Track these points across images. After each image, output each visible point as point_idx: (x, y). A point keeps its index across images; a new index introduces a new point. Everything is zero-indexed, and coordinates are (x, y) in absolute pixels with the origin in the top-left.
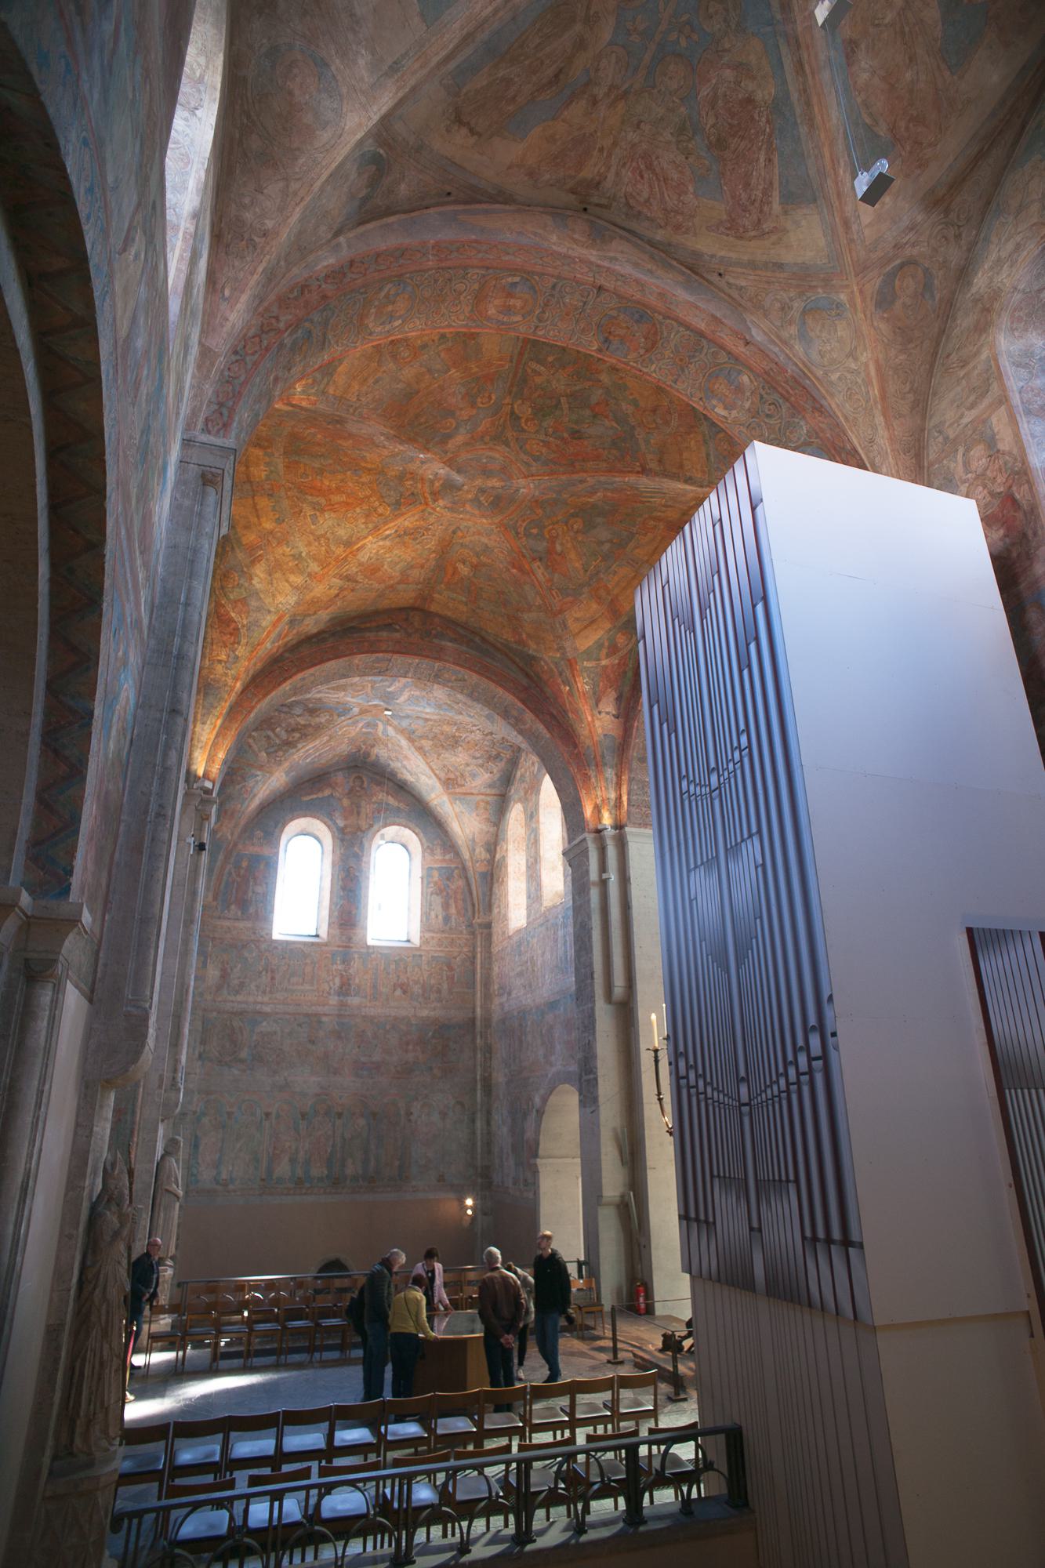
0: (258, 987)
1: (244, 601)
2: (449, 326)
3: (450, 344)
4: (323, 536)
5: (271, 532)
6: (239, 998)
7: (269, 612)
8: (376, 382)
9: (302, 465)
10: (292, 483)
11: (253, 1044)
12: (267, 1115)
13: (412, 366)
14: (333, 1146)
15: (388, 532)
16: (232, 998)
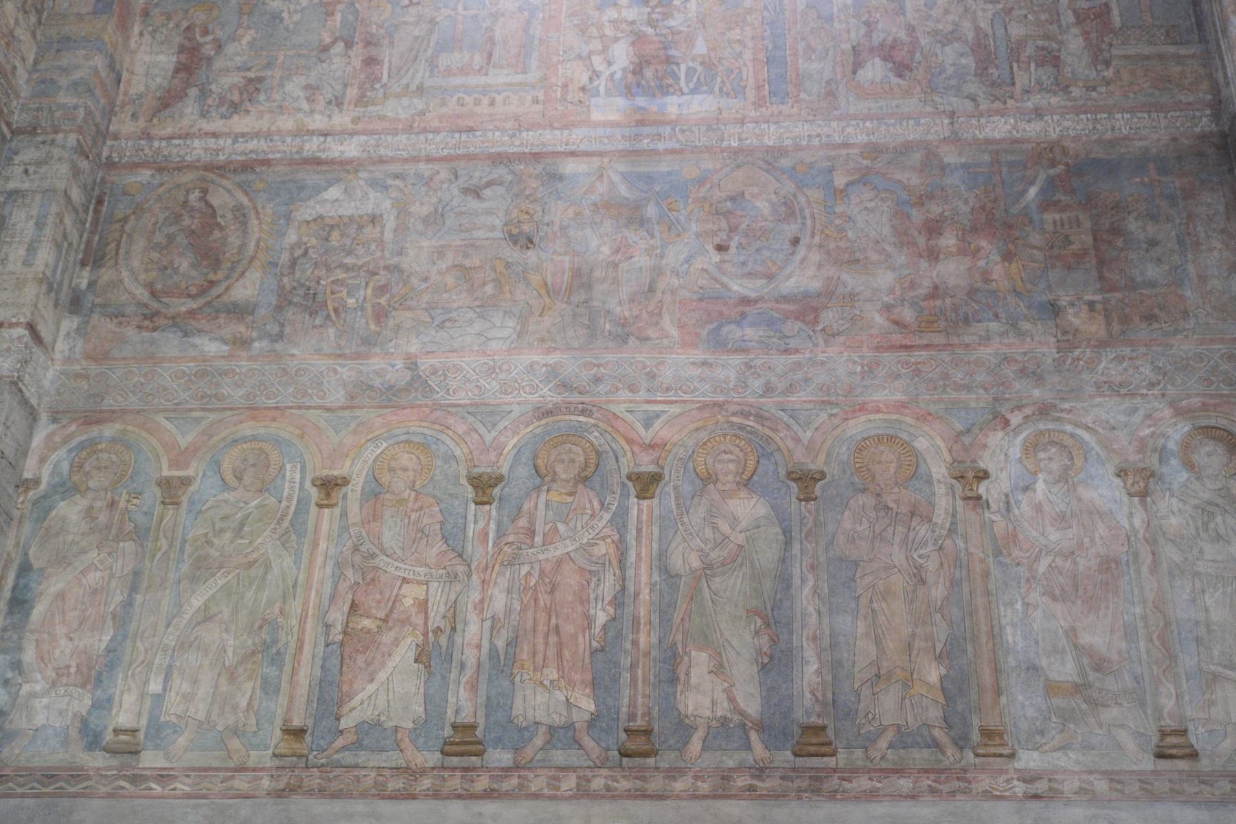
0: (312, 90)
6: (241, 123)
11: (285, 257)
12: (329, 486)
14: (618, 602)
16: (217, 125)
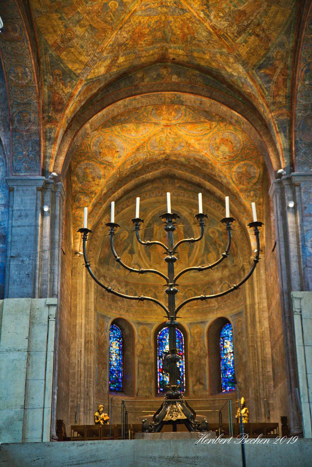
1: (243, 84)
2: (28, 48)
3: (64, 15)
4: (208, 41)
5: (211, 58)
7: (246, 78)
8: (82, 47)
9: (172, 39)
10: (183, 44)
13: (76, 31)
15: (202, 15)
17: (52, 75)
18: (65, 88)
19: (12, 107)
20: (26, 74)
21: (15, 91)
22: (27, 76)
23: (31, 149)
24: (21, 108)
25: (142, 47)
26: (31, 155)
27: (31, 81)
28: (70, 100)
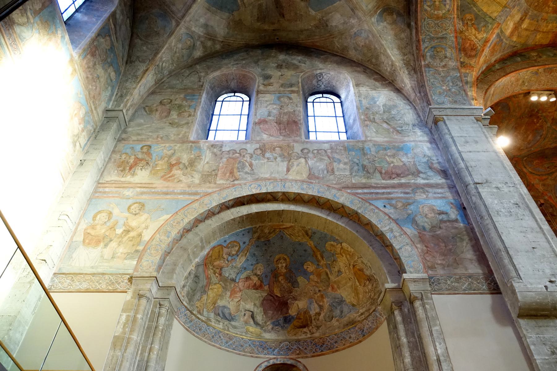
17: (462, 21)
18: (479, 33)
19: (424, 42)
20: (444, 3)
21: (428, 24)
22: (445, 5)
23: (451, 84)
24: (434, 43)
25: (547, 13)
26: (453, 90)
27: (449, 11)
28: (485, 46)
